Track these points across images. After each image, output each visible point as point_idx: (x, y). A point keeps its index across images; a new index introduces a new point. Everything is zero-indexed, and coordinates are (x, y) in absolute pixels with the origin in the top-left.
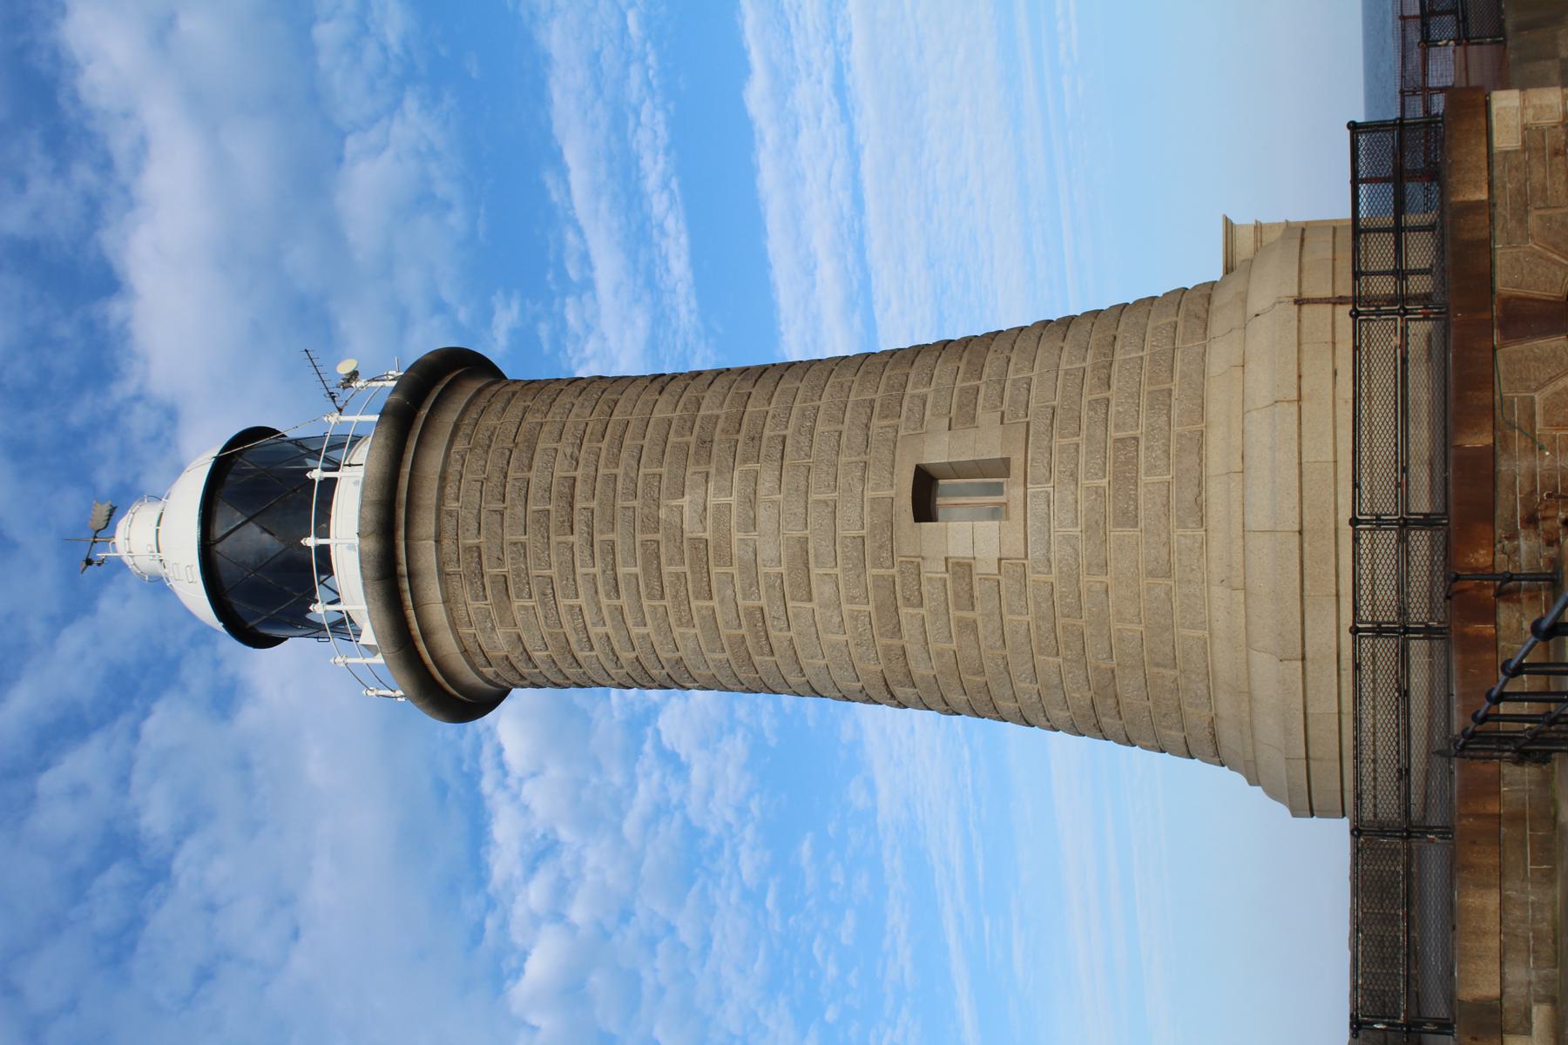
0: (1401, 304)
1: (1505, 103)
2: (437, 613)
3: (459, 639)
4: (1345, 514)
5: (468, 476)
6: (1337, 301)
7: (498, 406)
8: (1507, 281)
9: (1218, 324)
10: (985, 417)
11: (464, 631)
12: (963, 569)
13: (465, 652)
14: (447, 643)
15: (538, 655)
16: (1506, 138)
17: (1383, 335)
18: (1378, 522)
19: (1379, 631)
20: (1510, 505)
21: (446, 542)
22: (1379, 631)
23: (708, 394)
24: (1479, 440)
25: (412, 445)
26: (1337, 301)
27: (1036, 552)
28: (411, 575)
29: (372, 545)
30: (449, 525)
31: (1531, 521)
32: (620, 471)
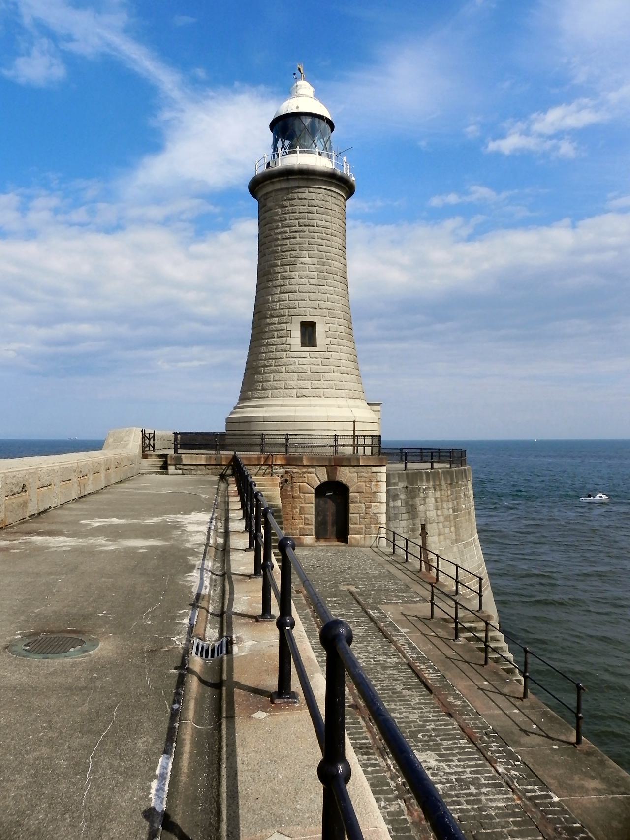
0: (355, 446)
2: (278, 186)
3: (271, 192)
4: (289, 432)
6: (354, 430)
9: (351, 402)
10: (327, 341)
11: (273, 194)
13: (267, 193)
14: (270, 188)
15: (267, 214)
16: (375, 469)
17: (331, 441)
18: (287, 439)
19: (262, 439)
22: (262, 439)
26: (354, 430)
27: (292, 354)
28: (288, 179)
29: (296, 167)
31: (287, 473)
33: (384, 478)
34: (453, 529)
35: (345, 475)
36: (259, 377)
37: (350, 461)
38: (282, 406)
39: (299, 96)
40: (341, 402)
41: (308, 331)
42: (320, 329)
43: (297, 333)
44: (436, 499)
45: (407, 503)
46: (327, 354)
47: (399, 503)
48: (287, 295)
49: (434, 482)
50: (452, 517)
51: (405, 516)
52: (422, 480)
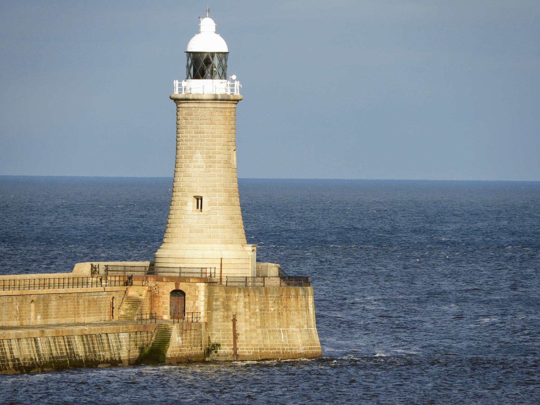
5: (205, 112)
7: (221, 114)
8: (181, 283)
10: (209, 208)
12: (186, 204)
16: (198, 284)
20: (157, 283)
21: (194, 109)
23: (222, 155)
24: (164, 280)
25: (211, 101)
30: (197, 109)
32: (205, 142)
34: (258, 320)
35: (183, 286)
45: (223, 303)
47: (219, 303)
50: (258, 314)
51: (222, 310)
52: (235, 292)
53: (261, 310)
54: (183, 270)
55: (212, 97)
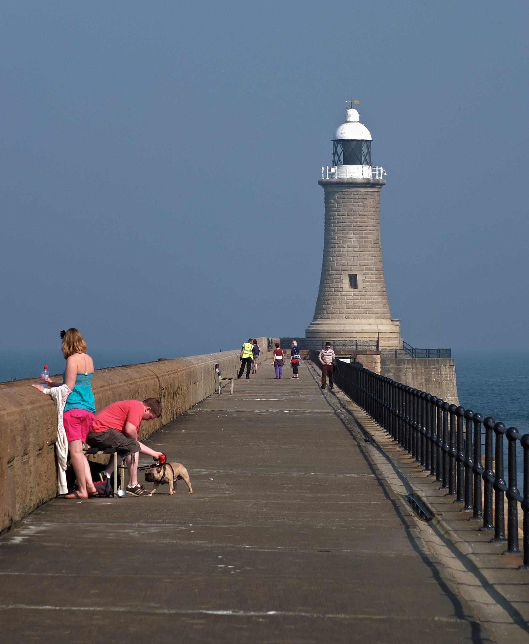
1: (379, 356)
8: (358, 356)
9: (378, 321)
12: (341, 282)
16: (374, 356)
33: (379, 361)
36: (325, 306)
37: (362, 353)
38: (337, 324)
39: (349, 122)
40: (372, 321)
41: (353, 280)
42: (359, 278)
43: (346, 282)
44: (413, 374)
45: (395, 375)
46: (364, 293)
48: (341, 258)
49: (412, 364)
52: (404, 363)
53: (426, 381)
54: (359, 344)
55: (366, 181)
